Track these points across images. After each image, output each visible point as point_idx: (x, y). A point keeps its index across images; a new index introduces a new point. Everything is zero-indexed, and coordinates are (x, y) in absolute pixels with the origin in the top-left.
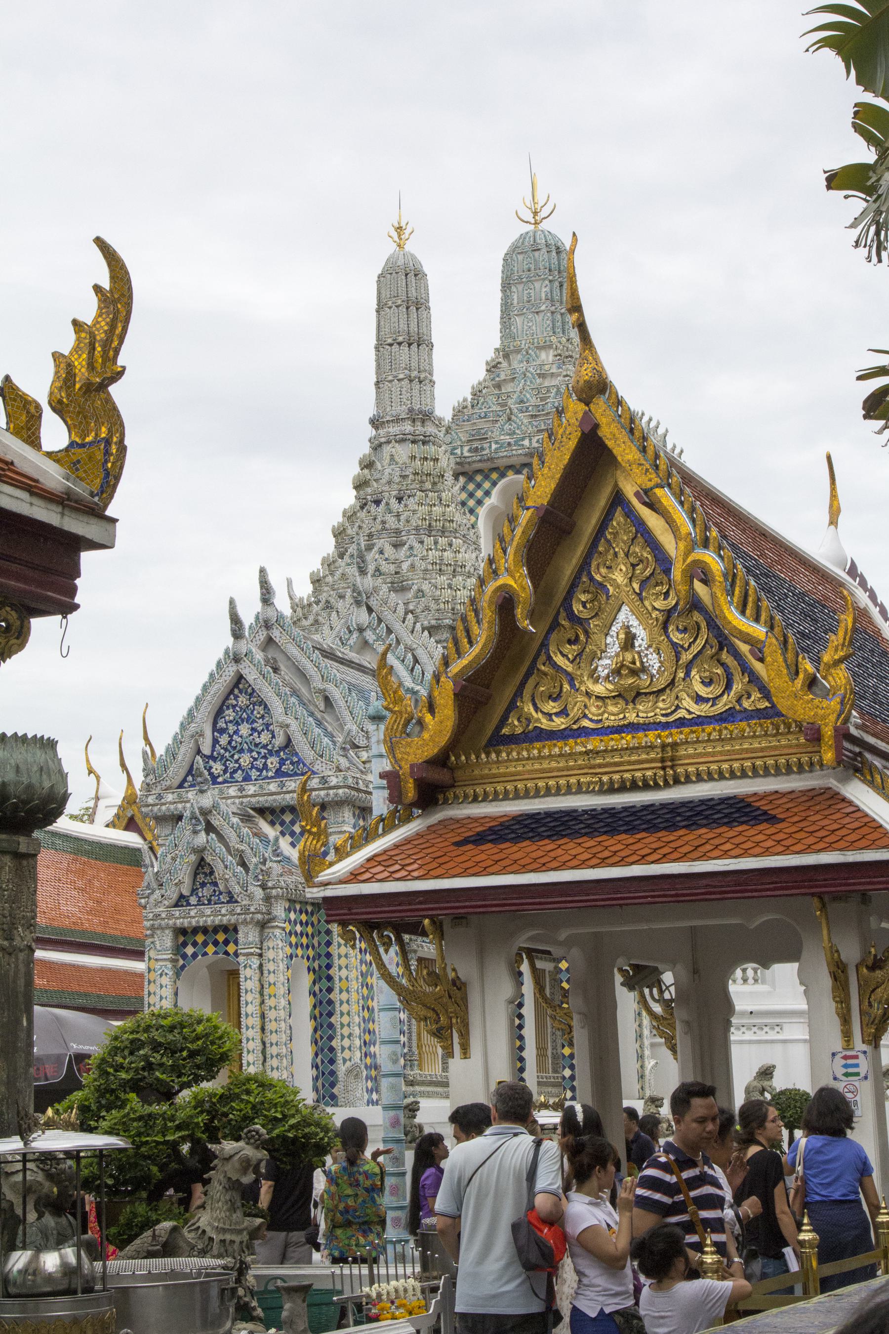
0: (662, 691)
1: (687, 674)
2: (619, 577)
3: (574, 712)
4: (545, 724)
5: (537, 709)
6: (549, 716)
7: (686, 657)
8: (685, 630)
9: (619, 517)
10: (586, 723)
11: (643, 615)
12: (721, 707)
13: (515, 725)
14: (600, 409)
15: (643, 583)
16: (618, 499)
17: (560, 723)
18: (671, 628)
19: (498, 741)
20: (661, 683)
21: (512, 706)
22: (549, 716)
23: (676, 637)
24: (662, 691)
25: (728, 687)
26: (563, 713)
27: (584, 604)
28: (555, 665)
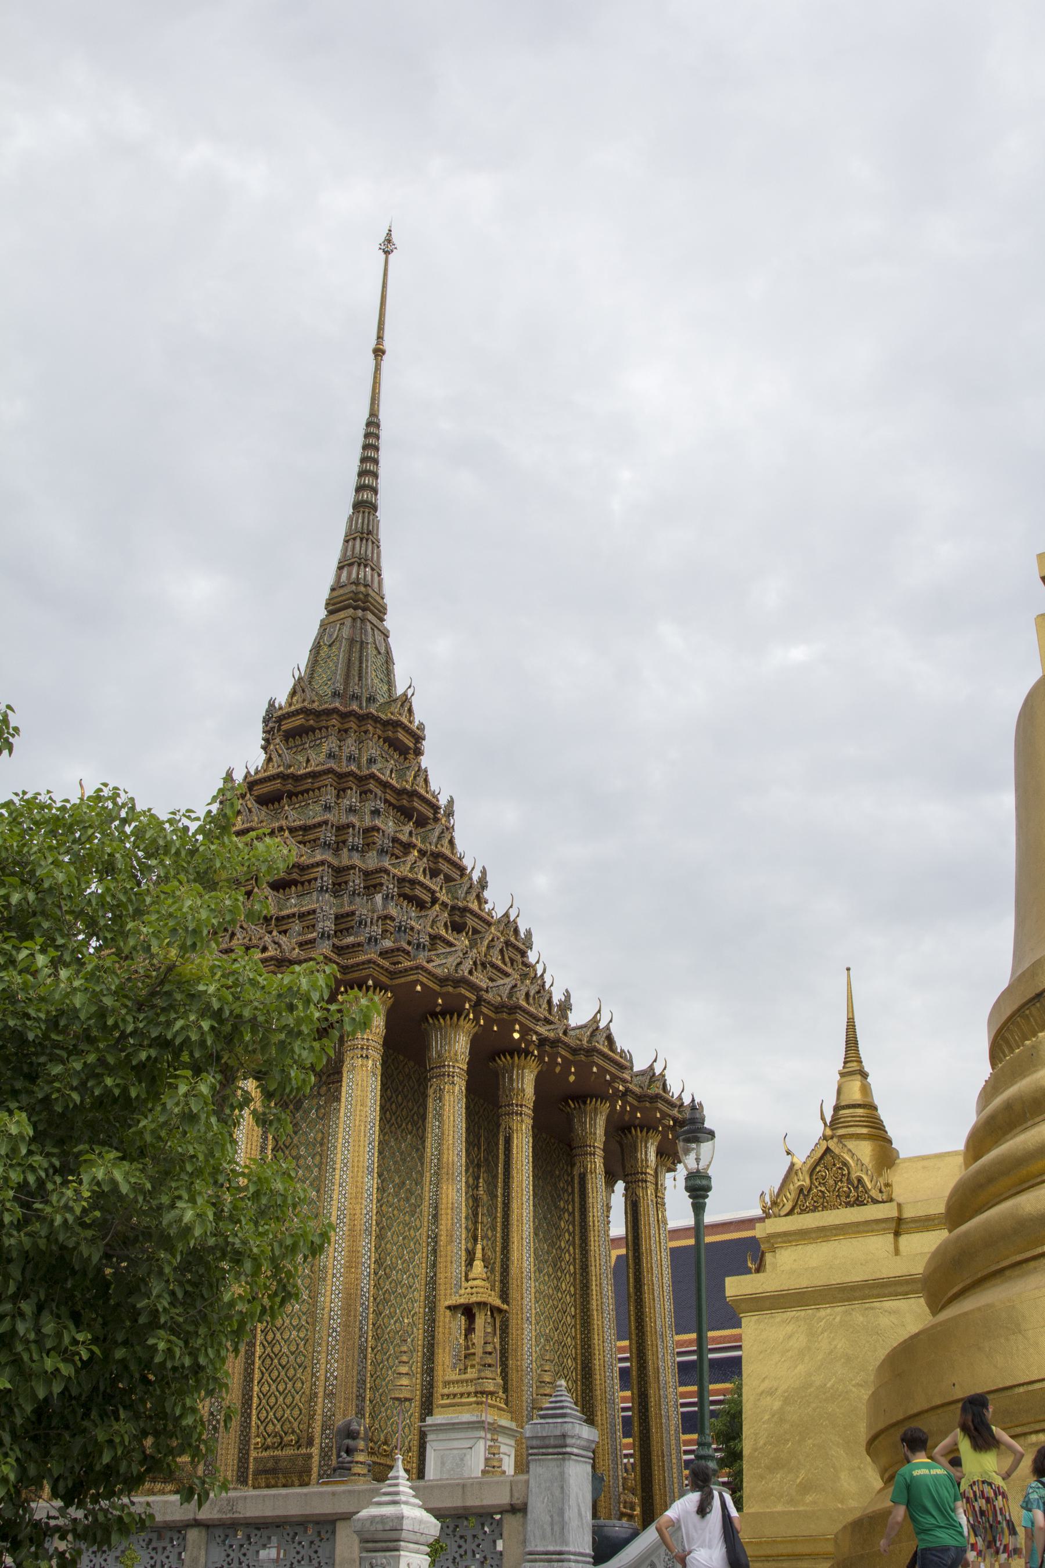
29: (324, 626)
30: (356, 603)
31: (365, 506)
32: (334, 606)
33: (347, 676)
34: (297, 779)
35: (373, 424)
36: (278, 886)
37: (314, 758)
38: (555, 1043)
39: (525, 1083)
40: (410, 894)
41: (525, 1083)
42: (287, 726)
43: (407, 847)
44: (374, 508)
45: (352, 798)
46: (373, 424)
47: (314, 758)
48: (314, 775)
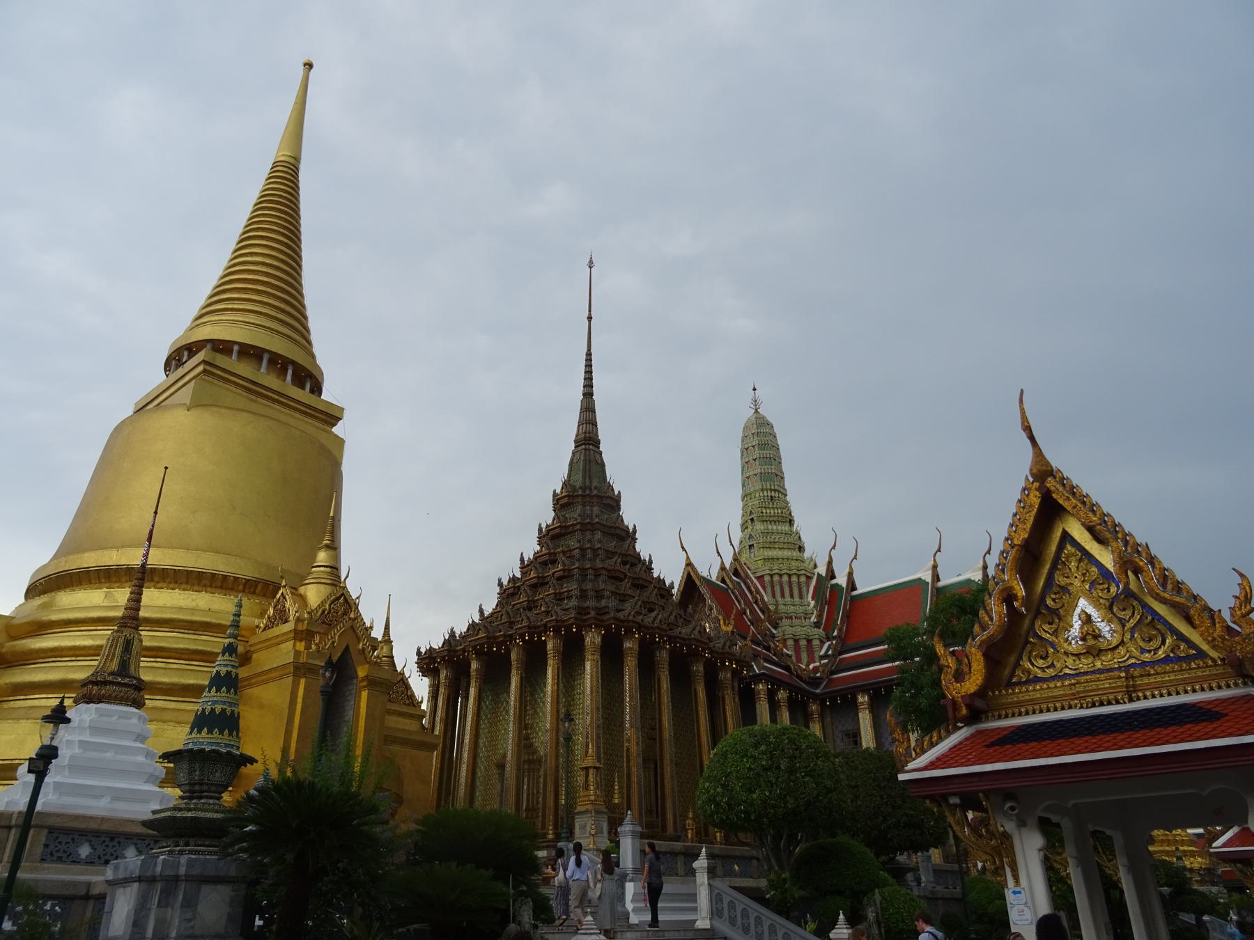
0: (1117, 647)
1: (1132, 636)
2: (1077, 583)
3: (1058, 665)
4: (1040, 674)
5: (1033, 665)
6: (1042, 669)
7: (1129, 626)
8: (1124, 610)
9: (1069, 548)
10: (1067, 671)
11: (1096, 603)
12: (1161, 654)
13: (1020, 675)
14: (1050, 483)
15: (1093, 584)
16: (1066, 536)
17: (1051, 672)
18: (1115, 609)
19: (1010, 684)
20: (1115, 642)
21: (1017, 665)
22: (1042, 669)
23: (1121, 614)
24: (1117, 647)
25: (1163, 642)
26: (1052, 665)
27: (1054, 600)
28: (1041, 638)
29: (574, 453)
30: (588, 441)
31: (588, 394)
32: (578, 443)
33: (584, 477)
34: (566, 527)
35: (589, 354)
36: (559, 579)
37: (574, 515)
38: (676, 637)
39: (663, 656)
40: (616, 578)
41: (663, 656)
42: (561, 502)
43: (614, 553)
44: (592, 394)
45: (588, 536)
46: (589, 354)
47: (574, 515)
48: (573, 525)
